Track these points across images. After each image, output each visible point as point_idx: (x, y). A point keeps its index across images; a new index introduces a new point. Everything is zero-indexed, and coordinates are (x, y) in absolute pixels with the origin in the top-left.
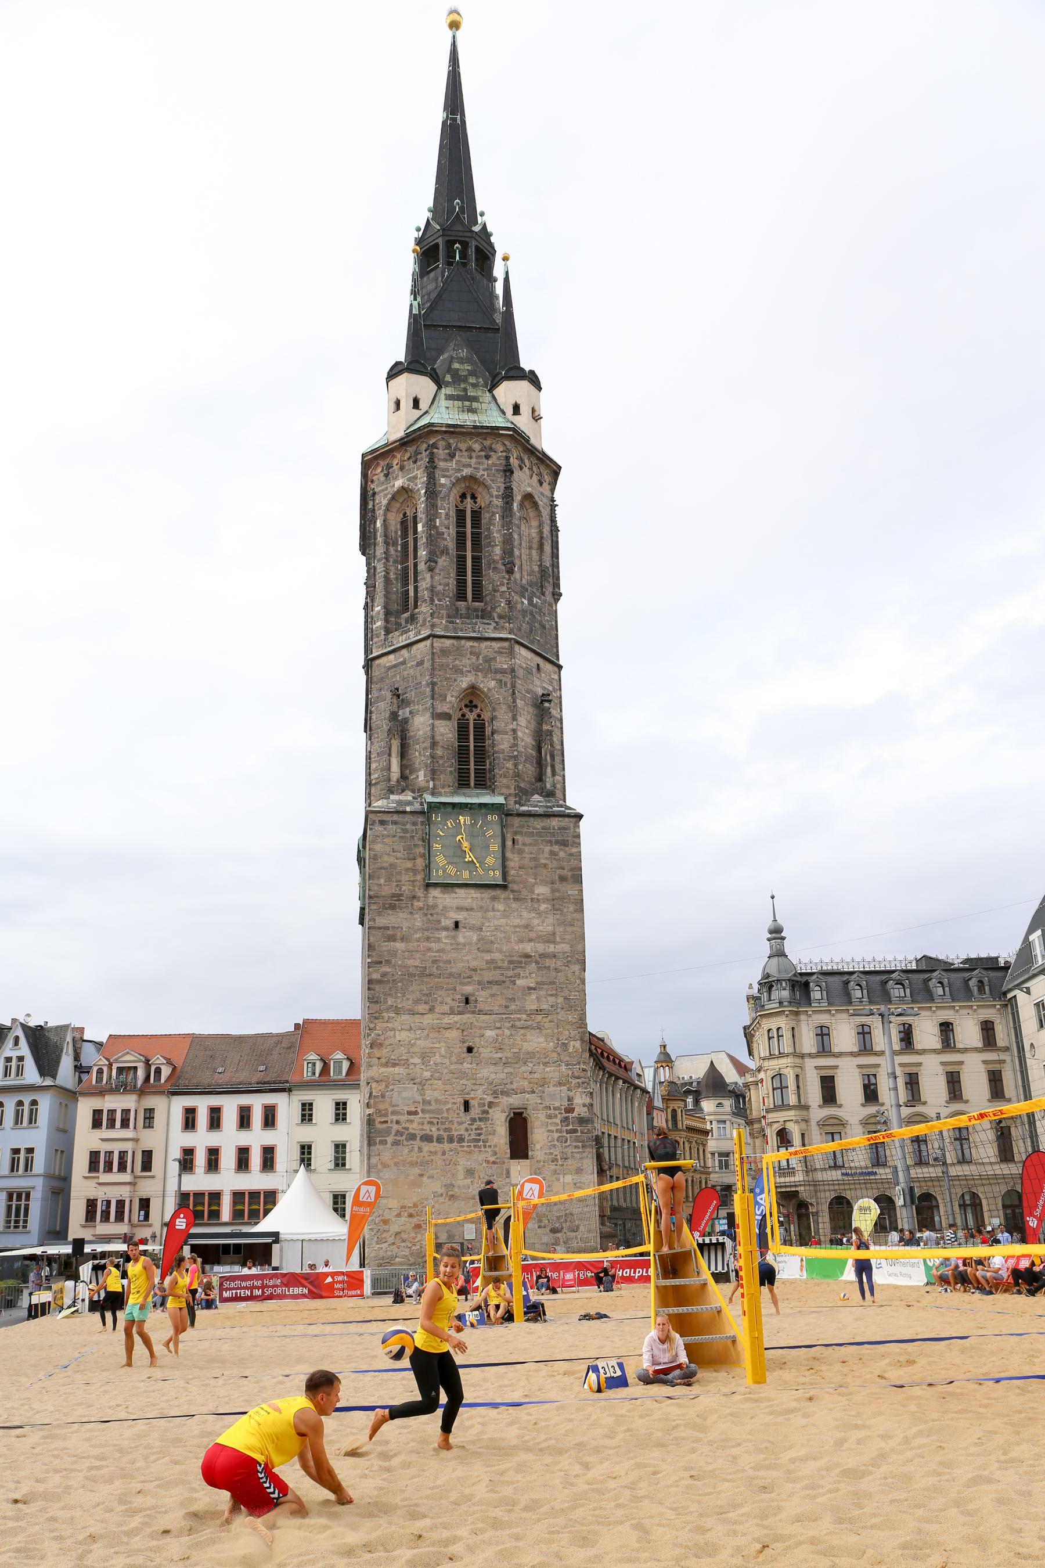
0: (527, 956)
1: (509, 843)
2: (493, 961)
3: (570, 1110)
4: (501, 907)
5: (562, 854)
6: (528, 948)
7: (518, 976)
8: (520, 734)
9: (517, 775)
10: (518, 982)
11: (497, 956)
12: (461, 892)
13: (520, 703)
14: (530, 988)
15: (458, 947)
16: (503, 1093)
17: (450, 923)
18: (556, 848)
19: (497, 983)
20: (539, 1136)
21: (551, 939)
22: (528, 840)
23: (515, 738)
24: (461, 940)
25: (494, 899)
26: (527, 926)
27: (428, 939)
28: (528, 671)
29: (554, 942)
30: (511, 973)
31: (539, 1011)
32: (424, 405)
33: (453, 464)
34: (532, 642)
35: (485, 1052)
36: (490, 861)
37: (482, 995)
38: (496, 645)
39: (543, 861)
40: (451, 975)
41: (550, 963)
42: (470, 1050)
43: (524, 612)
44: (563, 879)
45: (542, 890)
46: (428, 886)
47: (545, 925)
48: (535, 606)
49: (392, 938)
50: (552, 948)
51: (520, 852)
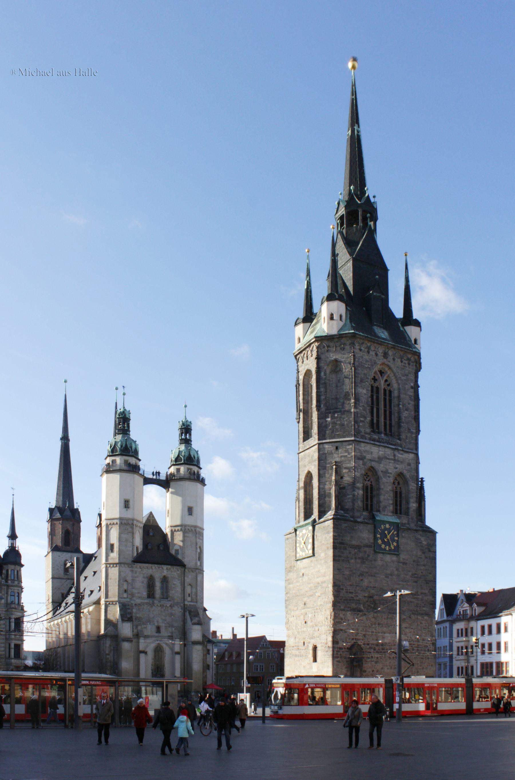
0: (318, 583)
2: (310, 588)
3: (326, 644)
4: (313, 565)
5: (328, 537)
6: (319, 580)
7: (316, 592)
10: (317, 594)
11: (312, 585)
14: (319, 596)
16: (312, 638)
19: (311, 596)
24: (304, 580)
26: (319, 571)
29: (324, 576)
30: (314, 591)
35: (309, 623)
39: (323, 542)
42: (306, 622)
48: (337, 418)
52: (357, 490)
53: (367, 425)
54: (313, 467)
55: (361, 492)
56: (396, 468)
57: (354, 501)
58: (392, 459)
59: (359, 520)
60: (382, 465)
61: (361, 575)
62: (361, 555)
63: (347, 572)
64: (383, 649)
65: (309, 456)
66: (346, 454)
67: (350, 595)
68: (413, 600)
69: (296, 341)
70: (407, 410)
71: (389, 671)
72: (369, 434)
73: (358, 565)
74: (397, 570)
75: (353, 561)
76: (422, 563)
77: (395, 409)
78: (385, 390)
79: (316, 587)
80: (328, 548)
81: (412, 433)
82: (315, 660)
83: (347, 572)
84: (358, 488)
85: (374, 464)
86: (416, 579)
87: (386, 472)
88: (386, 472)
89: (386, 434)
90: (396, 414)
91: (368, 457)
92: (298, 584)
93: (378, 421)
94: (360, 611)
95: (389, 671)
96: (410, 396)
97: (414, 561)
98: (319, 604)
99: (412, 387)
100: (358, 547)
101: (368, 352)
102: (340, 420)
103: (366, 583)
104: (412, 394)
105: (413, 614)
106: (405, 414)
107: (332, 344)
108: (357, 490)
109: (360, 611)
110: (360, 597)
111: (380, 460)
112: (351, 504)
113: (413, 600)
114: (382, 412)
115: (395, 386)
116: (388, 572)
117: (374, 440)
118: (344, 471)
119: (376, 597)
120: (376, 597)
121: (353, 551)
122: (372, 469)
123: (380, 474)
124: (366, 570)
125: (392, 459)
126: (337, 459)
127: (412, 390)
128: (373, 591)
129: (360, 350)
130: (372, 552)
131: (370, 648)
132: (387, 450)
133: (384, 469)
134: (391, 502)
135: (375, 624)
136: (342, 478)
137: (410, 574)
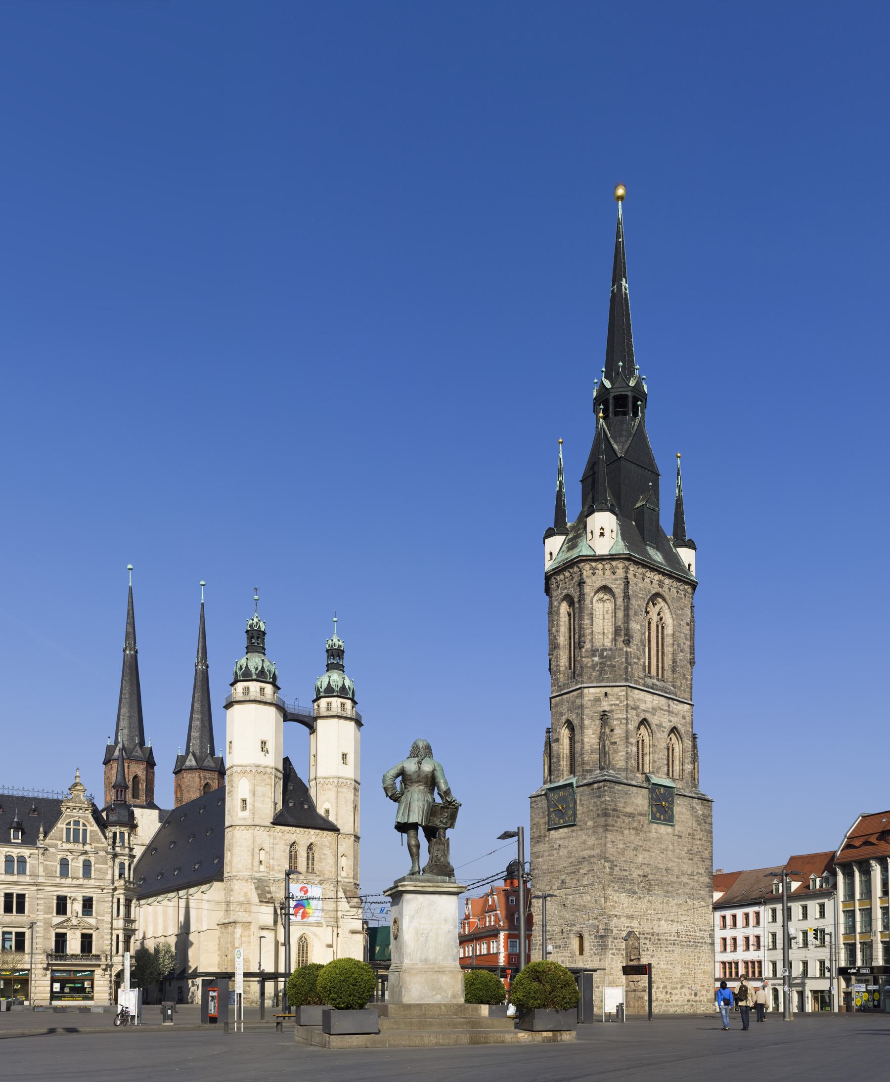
0: (584, 858)
1: (578, 801)
2: (571, 863)
3: (598, 932)
4: (574, 834)
6: (586, 853)
8: (586, 740)
9: (583, 763)
11: (573, 860)
12: (561, 830)
13: (586, 722)
15: (560, 857)
16: (575, 925)
17: (556, 846)
18: (596, 800)
20: (586, 945)
21: (593, 848)
22: (586, 798)
23: (583, 744)
25: (572, 831)
26: (584, 842)
27: (550, 855)
28: (597, 700)
31: (587, 885)
32: (554, 556)
33: (560, 591)
34: (602, 681)
36: (570, 812)
37: (568, 880)
38: (575, 693)
40: (558, 871)
41: (592, 860)
43: (594, 666)
44: (598, 815)
45: (590, 823)
46: (549, 830)
47: (591, 841)
48: (606, 657)
49: (538, 857)
50: (592, 853)
51: (583, 805)
52: (630, 746)
53: (641, 668)
54: (574, 716)
55: (634, 749)
56: (671, 721)
57: (627, 759)
58: (666, 710)
59: (634, 783)
60: (656, 717)
61: (635, 849)
62: (635, 825)
63: (621, 846)
64: (659, 940)
65: (568, 702)
66: (618, 702)
67: (625, 873)
68: (689, 881)
69: (548, 557)
70: (682, 651)
71: (665, 966)
72: (643, 679)
73: (633, 837)
74: (673, 844)
75: (626, 832)
76: (698, 837)
77: (668, 650)
78: (657, 626)
79: (580, 863)
80: (598, 815)
81: (687, 679)
82: (581, 952)
83: (621, 846)
84: (632, 744)
85: (648, 716)
86: (691, 856)
87: (659, 726)
88: (659, 726)
89: (658, 680)
90: (670, 656)
91: (642, 706)
92: (552, 858)
93: (650, 663)
94: (635, 893)
95: (665, 966)
96: (686, 635)
97: (689, 834)
98: (585, 883)
99: (688, 624)
100: (631, 815)
101: (643, 579)
102: (610, 661)
103: (640, 860)
104: (688, 632)
105: (689, 898)
106: (681, 656)
107: (600, 566)
108: (630, 746)
109: (635, 893)
110: (635, 875)
111: (654, 711)
112: (624, 763)
113: (689, 881)
114: (654, 652)
115: (668, 620)
116: (663, 847)
117: (648, 687)
118: (615, 722)
119: (650, 877)
120: (650, 877)
121: (627, 820)
122: (645, 720)
123: (654, 727)
124: (640, 843)
125: (666, 710)
126: (607, 708)
127: (688, 628)
128: (648, 870)
129: (635, 575)
130: (647, 822)
131: (646, 938)
132: (661, 698)
133: (658, 722)
134: (666, 762)
135: (650, 909)
136: (612, 730)
137: (686, 849)
